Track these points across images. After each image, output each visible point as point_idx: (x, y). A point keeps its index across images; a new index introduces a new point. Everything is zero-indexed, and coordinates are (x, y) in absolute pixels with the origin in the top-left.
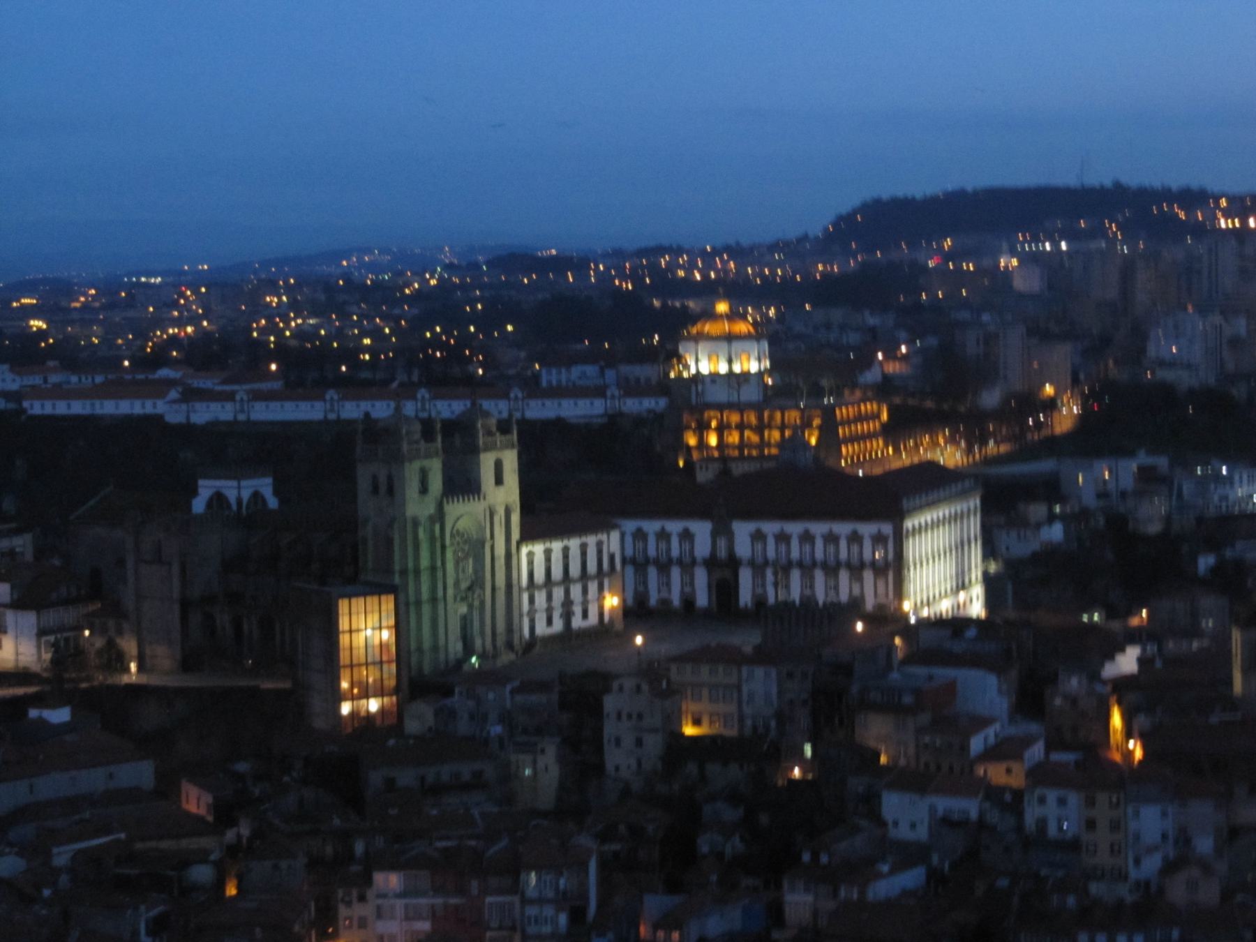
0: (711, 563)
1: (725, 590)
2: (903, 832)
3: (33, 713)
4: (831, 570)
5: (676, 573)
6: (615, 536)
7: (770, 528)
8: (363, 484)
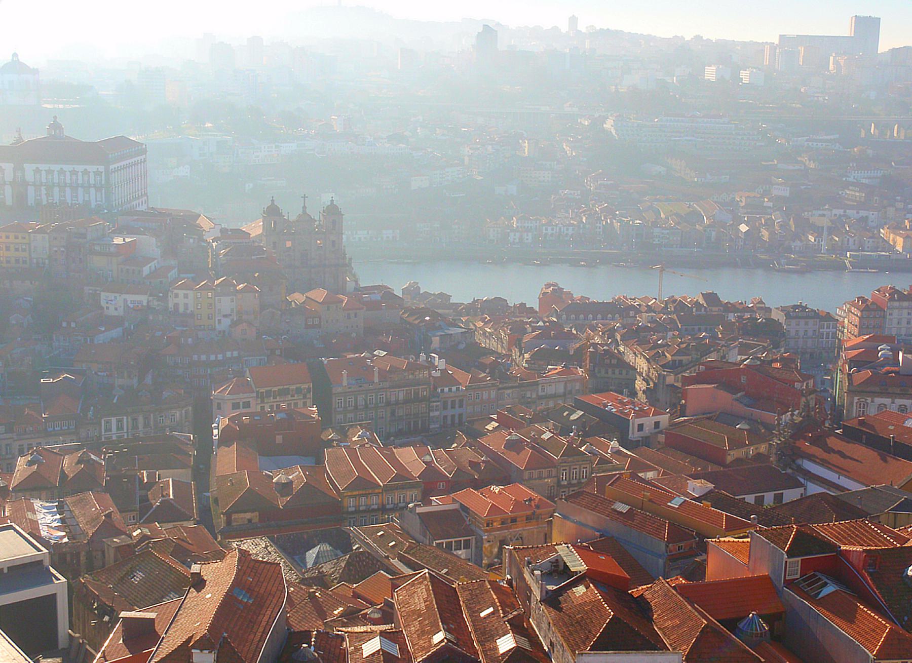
2: (112, 312)
7: (44, 167)
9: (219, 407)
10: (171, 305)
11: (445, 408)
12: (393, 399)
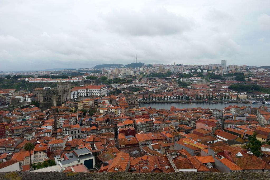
0: (86, 93)
1: (87, 95)
2: (101, 113)
3: (30, 106)
4: (96, 93)
5: (83, 93)
6: (79, 91)
8: (58, 87)
9: (119, 127)
10: (111, 111)
11: (155, 127)
12: (147, 126)
